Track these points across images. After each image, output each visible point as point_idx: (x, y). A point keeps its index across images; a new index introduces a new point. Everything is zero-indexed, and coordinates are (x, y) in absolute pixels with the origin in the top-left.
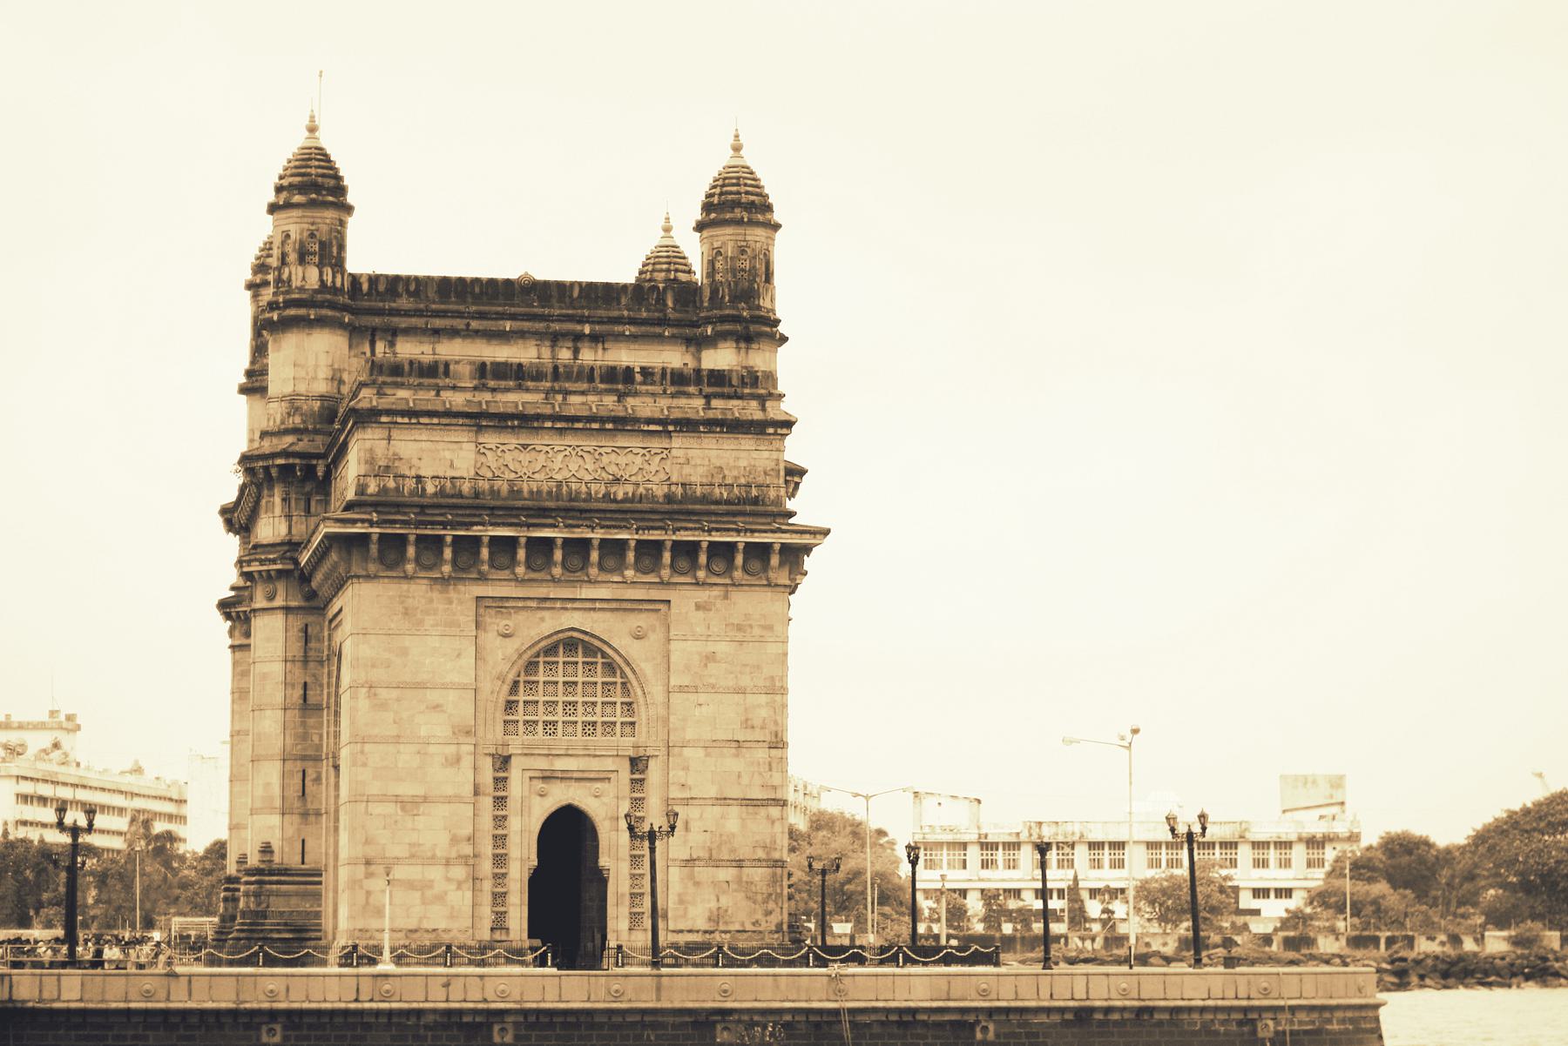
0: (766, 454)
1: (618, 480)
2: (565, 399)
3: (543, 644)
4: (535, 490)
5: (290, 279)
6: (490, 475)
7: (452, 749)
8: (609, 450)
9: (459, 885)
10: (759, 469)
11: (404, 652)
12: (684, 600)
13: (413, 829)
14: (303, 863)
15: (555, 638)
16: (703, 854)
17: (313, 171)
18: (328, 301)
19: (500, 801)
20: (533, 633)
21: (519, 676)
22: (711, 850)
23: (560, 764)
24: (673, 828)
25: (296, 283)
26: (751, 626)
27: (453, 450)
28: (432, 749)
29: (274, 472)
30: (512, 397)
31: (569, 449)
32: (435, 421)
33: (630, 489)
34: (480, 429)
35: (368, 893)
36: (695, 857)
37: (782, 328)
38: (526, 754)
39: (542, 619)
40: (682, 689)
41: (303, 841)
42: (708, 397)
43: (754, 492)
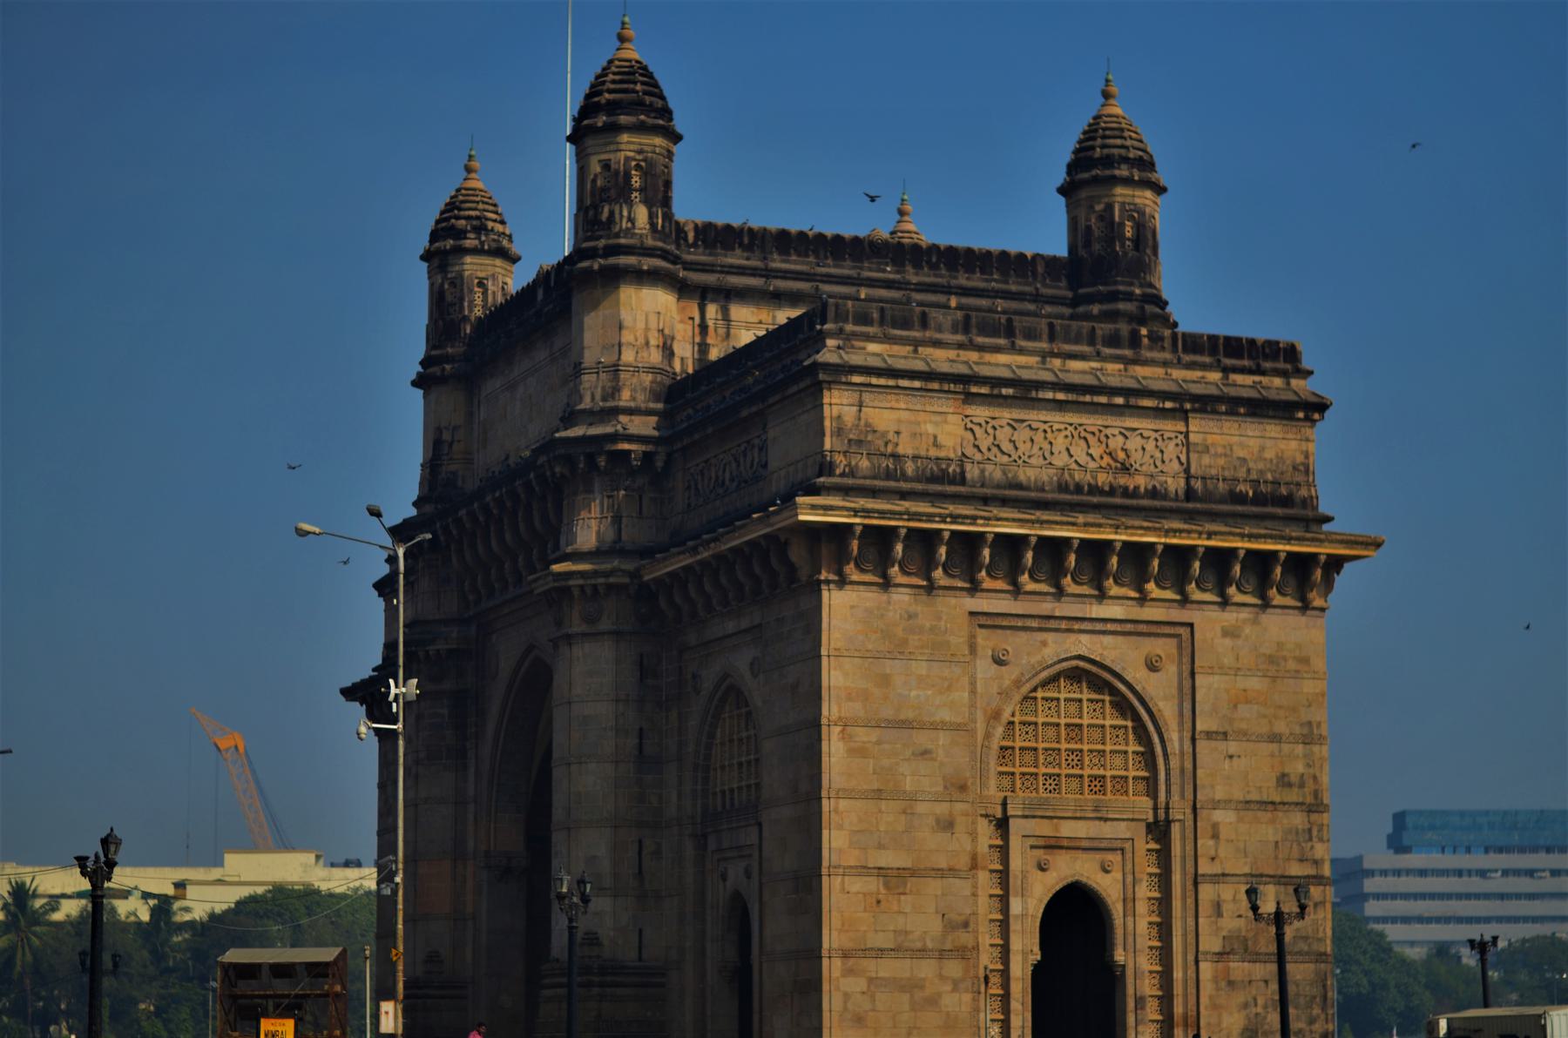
0: (1294, 444)
1: (1128, 469)
3: (1045, 674)
6: (978, 457)
7: (942, 809)
8: (1116, 432)
10: (1288, 462)
11: (885, 681)
12: (1210, 621)
13: (900, 912)
14: (640, 959)
15: (1058, 667)
17: (639, 87)
18: (661, 249)
19: (1004, 876)
20: (1033, 660)
21: (1013, 715)
23: (1068, 829)
26: (1285, 659)
27: (936, 424)
28: (921, 808)
29: (602, 462)
30: (1002, 358)
31: (1070, 428)
32: (917, 384)
34: (969, 398)
39: (1044, 644)
40: (1209, 735)
41: (640, 931)
42: (1226, 371)
43: (1284, 491)
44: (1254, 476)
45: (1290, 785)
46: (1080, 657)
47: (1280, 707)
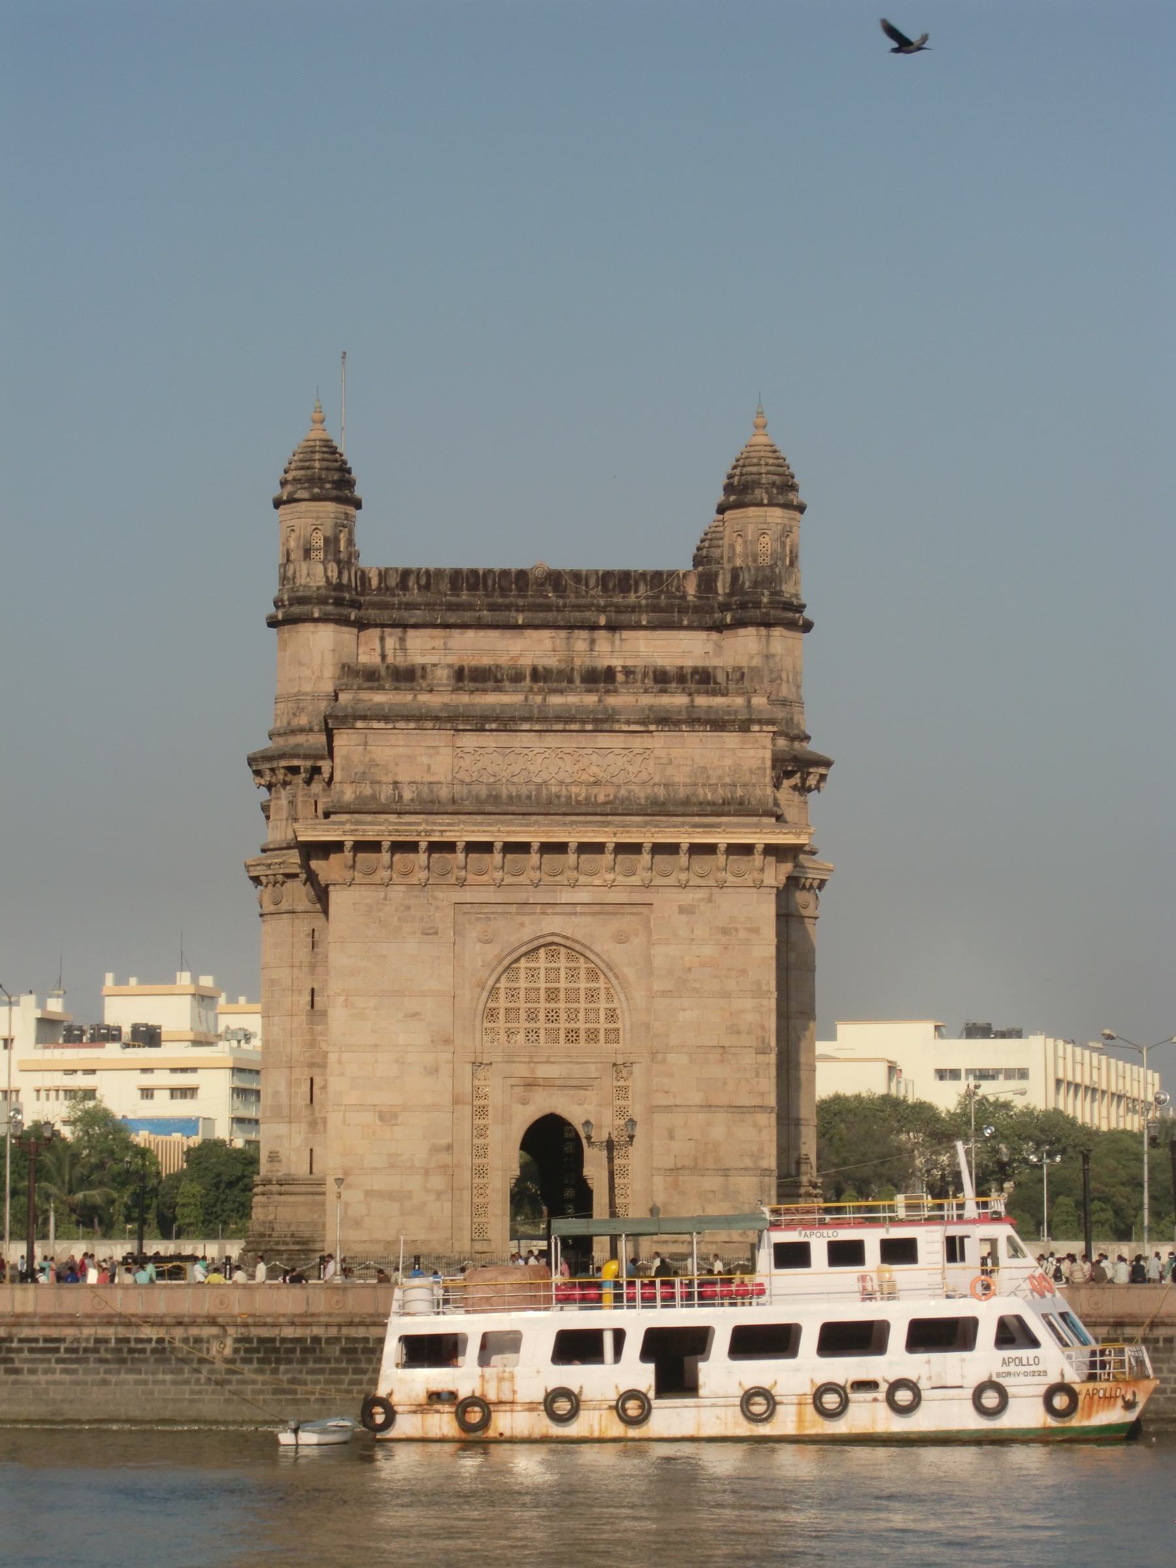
0: (752, 753)
2: (544, 700)
3: (524, 949)
4: (514, 794)
5: (294, 577)
6: (468, 780)
9: (439, 1195)
12: (667, 901)
14: (311, 1172)
16: (687, 1163)
22: (696, 1159)
23: (543, 1071)
24: (632, 1137)
25: (302, 580)
26: (736, 930)
27: (431, 756)
31: (549, 751)
33: (611, 791)
35: (347, 1205)
36: (679, 1165)
37: (807, 614)
38: (506, 1062)
39: (522, 925)
40: (665, 994)
41: (311, 1150)
42: (690, 695)
43: (739, 792)
44: (713, 781)
45: (738, 1033)
46: (552, 934)
47: (732, 969)
